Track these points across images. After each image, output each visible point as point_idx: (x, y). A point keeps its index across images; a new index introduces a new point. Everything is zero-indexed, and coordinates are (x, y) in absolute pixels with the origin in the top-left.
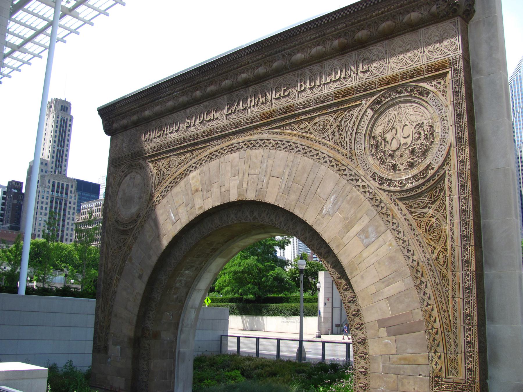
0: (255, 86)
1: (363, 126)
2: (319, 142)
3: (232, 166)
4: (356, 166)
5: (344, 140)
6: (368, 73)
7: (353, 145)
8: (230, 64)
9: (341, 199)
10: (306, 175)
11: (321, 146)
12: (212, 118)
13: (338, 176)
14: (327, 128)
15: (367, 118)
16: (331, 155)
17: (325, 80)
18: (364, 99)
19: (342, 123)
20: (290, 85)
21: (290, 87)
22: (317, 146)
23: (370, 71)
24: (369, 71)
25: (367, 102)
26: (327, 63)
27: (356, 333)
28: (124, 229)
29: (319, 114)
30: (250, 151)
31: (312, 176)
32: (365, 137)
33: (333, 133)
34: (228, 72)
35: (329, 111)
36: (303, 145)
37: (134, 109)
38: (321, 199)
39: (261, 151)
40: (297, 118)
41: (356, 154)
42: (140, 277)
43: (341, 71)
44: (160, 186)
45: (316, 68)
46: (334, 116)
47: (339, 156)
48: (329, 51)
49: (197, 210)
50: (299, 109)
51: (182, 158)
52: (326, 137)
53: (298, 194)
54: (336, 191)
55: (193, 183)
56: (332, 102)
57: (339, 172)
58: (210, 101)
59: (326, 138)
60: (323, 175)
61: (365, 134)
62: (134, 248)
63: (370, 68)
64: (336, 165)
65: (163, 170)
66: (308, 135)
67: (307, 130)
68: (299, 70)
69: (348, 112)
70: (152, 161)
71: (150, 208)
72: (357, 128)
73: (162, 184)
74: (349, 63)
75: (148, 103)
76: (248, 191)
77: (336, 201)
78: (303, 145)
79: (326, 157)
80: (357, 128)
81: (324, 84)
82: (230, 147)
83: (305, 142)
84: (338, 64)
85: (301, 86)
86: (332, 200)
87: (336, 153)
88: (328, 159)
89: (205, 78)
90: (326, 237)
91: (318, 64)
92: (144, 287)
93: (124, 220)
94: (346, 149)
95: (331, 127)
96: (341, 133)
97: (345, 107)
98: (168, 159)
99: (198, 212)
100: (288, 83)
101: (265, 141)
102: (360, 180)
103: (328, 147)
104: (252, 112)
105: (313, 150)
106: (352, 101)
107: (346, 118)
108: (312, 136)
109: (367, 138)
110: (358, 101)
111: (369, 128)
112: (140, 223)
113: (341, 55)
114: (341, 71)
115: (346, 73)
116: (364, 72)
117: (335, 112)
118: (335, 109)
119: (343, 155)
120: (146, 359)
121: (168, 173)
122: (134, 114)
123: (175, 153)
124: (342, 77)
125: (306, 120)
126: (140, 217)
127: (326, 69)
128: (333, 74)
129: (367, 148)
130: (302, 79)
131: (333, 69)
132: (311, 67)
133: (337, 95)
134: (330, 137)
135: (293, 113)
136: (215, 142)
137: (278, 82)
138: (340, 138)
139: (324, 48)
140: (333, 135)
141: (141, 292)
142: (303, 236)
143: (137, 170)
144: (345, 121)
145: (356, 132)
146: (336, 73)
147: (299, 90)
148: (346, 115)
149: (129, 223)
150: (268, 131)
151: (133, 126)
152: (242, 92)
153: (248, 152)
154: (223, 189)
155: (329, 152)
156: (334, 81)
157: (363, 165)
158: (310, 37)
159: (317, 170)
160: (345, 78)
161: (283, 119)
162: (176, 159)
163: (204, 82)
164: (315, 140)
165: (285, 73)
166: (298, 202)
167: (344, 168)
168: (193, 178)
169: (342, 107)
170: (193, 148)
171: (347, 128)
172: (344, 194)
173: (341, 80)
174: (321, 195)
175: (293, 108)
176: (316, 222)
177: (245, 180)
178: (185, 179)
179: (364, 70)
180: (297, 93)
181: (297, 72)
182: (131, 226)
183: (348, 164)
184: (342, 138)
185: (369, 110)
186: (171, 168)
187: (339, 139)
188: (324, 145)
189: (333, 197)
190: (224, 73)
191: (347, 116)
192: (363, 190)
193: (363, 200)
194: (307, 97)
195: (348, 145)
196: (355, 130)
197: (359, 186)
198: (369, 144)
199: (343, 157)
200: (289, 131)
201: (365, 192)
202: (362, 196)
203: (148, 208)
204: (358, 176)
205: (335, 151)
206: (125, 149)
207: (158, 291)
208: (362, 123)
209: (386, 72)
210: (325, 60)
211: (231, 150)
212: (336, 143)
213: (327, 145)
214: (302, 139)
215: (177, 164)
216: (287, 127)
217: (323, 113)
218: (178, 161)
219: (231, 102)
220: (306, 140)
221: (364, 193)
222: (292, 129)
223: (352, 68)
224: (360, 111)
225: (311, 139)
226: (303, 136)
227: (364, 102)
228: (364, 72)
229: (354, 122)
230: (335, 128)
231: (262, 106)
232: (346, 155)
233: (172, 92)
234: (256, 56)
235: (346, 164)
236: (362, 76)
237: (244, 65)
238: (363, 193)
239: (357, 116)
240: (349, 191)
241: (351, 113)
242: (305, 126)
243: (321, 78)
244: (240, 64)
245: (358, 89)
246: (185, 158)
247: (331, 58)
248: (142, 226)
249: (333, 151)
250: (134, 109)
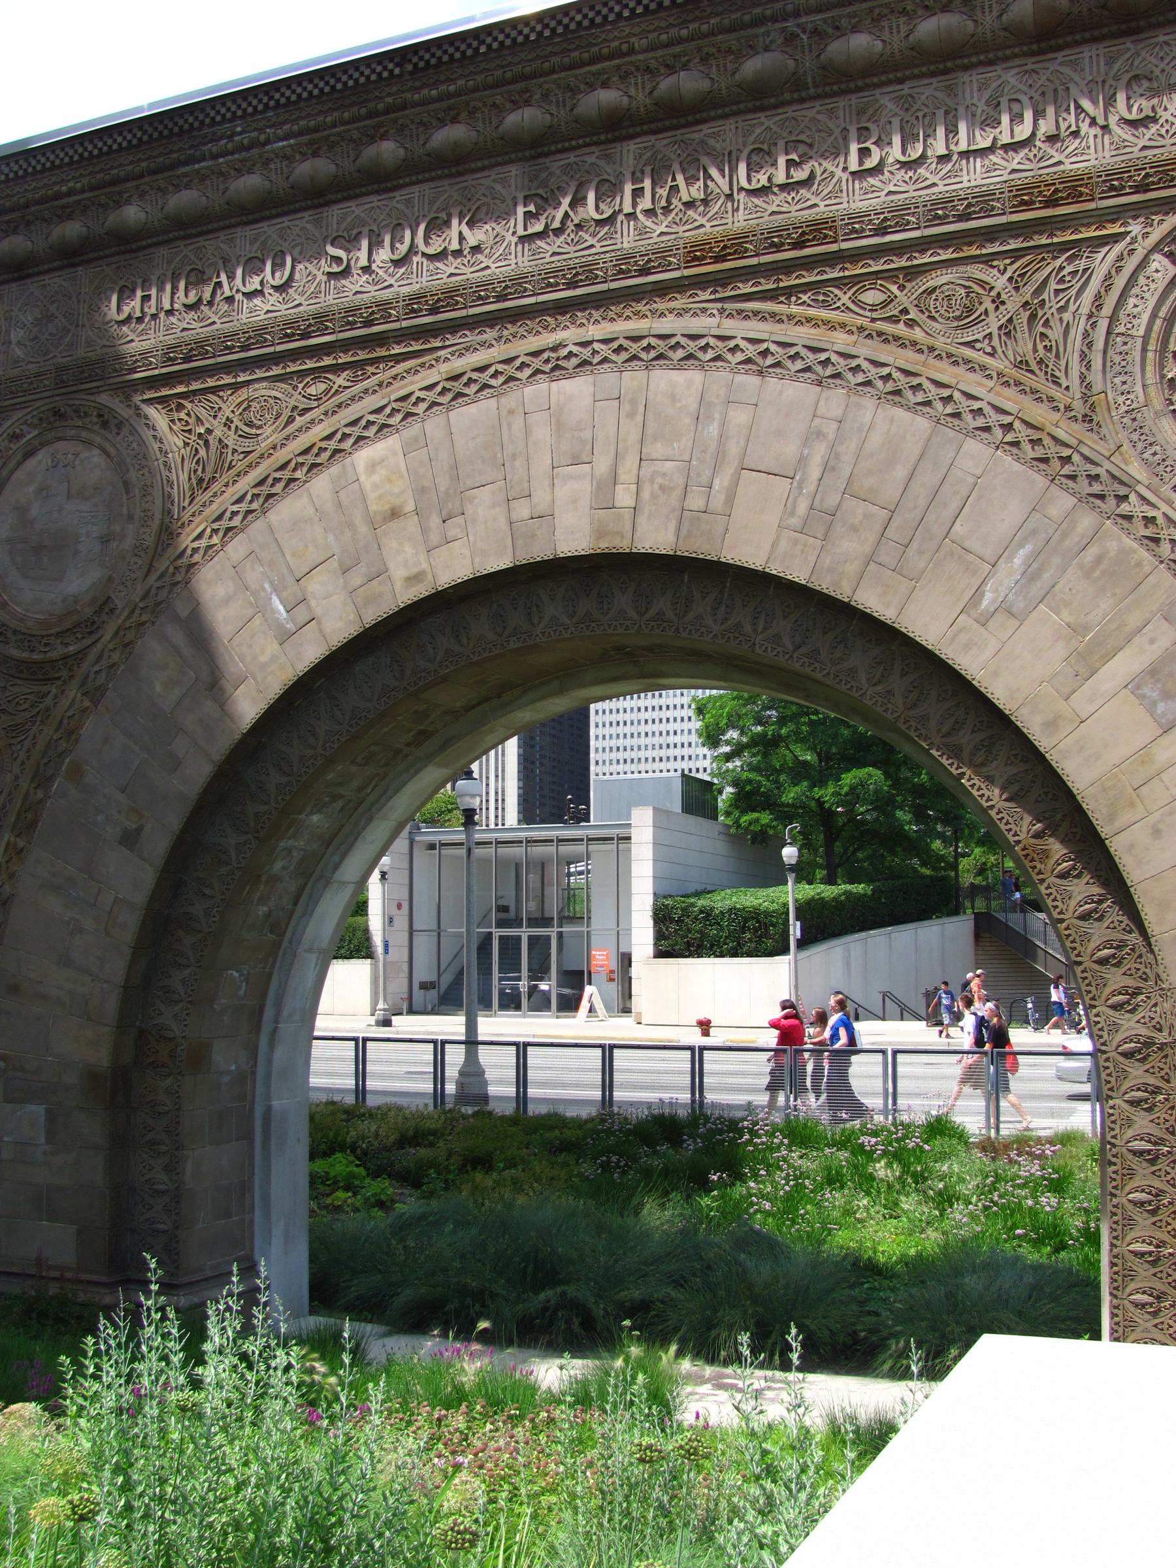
0: (652, 138)
1: (1135, 311)
2: (950, 355)
3: (559, 427)
4: (1113, 447)
5: (1057, 356)
6: (1154, 128)
7: (1095, 377)
8: (549, 49)
9: (1056, 560)
10: (900, 473)
11: (961, 370)
12: (455, 246)
13: (1040, 481)
14: (981, 309)
15: (1153, 286)
16: (1008, 406)
17: (971, 139)
18: (1135, 218)
19: (1045, 296)
20: (811, 146)
21: (811, 153)
22: (946, 372)
23: (1161, 121)
24: (1154, 120)
25: (1148, 229)
26: (974, 78)
27: (1115, 1024)
28: (35, 656)
29: (944, 257)
30: (642, 374)
31: (927, 479)
32: (1144, 350)
33: (1008, 330)
34: (533, 76)
35: (990, 251)
36: (884, 365)
37: (69, 194)
38: (970, 557)
39: (695, 377)
40: (848, 265)
41: (1113, 406)
42: (130, 839)
43: (1038, 114)
44: (210, 493)
45: (927, 91)
46: (1010, 270)
47: (1040, 411)
48: (989, 35)
49: (399, 586)
50: (859, 234)
51: (312, 390)
52: (977, 341)
53: (871, 537)
54: (1034, 533)
55: (376, 487)
56: (1003, 220)
57: (1042, 466)
58: (439, 183)
59: (978, 346)
60: (978, 472)
61: (1146, 338)
62: (90, 728)
63: (1160, 112)
64: (1031, 441)
65: (218, 433)
66: (900, 329)
67: (896, 312)
68: (853, 97)
69: (1070, 259)
70: (162, 400)
71: (161, 576)
72: (1113, 318)
73: (215, 487)
74: (1072, 86)
75: (142, 176)
76: (642, 521)
77: (1035, 566)
78: (884, 365)
79: (987, 410)
80: (1113, 318)
81: (966, 155)
82: (545, 356)
83: (886, 354)
84: (1021, 86)
85: (864, 153)
86: (1017, 561)
87: (1027, 401)
88: (993, 418)
89: (425, 92)
90: (999, 692)
91: (934, 80)
92: (149, 876)
93: (30, 623)
94: (1067, 388)
95: (997, 308)
96: (1043, 330)
97: (1055, 240)
98: (243, 394)
99: (406, 596)
100: (802, 137)
101: (712, 341)
102: (1133, 497)
103: (989, 377)
104: (642, 232)
105: (927, 384)
106: (1086, 221)
107: (1061, 281)
108: (918, 334)
109: (1150, 355)
110: (1108, 225)
111: (1158, 322)
112: (117, 633)
113: (1033, 54)
114: (1038, 114)
115: (1057, 122)
116: (1133, 124)
117: (1016, 254)
118: (1013, 245)
119: (1056, 409)
120: (163, 1148)
121: (247, 445)
122: (66, 214)
123: (276, 371)
124: (1040, 134)
125: (889, 275)
126: (112, 611)
127: (968, 102)
128: (1005, 119)
129: (1152, 391)
130: (867, 129)
131: (1004, 101)
132: (906, 88)
133: (1023, 196)
134: (995, 342)
135: (834, 247)
136: (472, 337)
137: (758, 131)
138: (1040, 347)
139: (970, 23)
140: (1008, 334)
141: (140, 898)
142: (879, 688)
143: (84, 434)
144: (1057, 292)
145: (1109, 333)
146: (1017, 118)
147: (854, 166)
148: (1061, 268)
149: (58, 635)
150: (719, 305)
151: (56, 264)
152: (590, 159)
153: (633, 379)
154: (522, 510)
155: (998, 394)
156: (1006, 147)
157: (1140, 445)
158: (655, 35)
159: (952, 455)
160: (1052, 139)
161: (788, 267)
162: (279, 395)
163: (418, 109)
164: (932, 349)
165: (789, 103)
166: (872, 566)
167: (1066, 452)
168: (372, 466)
169: (1044, 241)
170: (362, 355)
171: (1067, 316)
172: (1068, 543)
173: (1038, 143)
174: (971, 544)
175: (830, 228)
176: (955, 636)
177: (622, 477)
178: (334, 470)
179: (1134, 116)
180: (845, 176)
181: (842, 102)
182: (67, 645)
183: (1080, 442)
184: (1048, 349)
185: (1157, 256)
186: (259, 427)
187: (1035, 350)
188: (972, 369)
189: (1021, 552)
190: (514, 81)
191: (1065, 272)
192: (1148, 533)
193: (1147, 569)
194: (890, 193)
195: (1075, 372)
196: (1103, 325)
197: (1128, 518)
198: (1162, 376)
199: (1056, 416)
200: (812, 312)
201: (1156, 541)
202: (1143, 553)
203: (153, 577)
204: (1122, 483)
205: (1023, 392)
206: (20, 353)
207: (208, 891)
208: (1132, 301)
209: (1093, 156)
210: (966, 68)
211: (553, 370)
212: (1023, 365)
213: (983, 368)
214: (875, 343)
215: (286, 413)
216: (804, 298)
217: (961, 255)
218: (293, 403)
219: (540, 191)
220: (891, 347)
221: (1151, 545)
222: (825, 305)
223: (1086, 104)
224: (1120, 258)
225: (914, 343)
226: (880, 334)
227: (1135, 228)
228: (1133, 124)
229: (1098, 296)
230: (1017, 313)
231: (690, 213)
232: (1068, 408)
233: (262, 138)
234: (671, 26)
235: (1074, 442)
236: (1125, 137)
237: (611, 57)
238: (1146, 541)
239: (1108, 276)
240: (1090, 533)
241: (1082, 264)
242: (882, 297)
243: (952, 131)
244: (595, 49)
245: (1113, 182)
246: (327, 391)
247: (991, 63)
248: (126, 645)
249: (1011, 392)
250: (69, 194)
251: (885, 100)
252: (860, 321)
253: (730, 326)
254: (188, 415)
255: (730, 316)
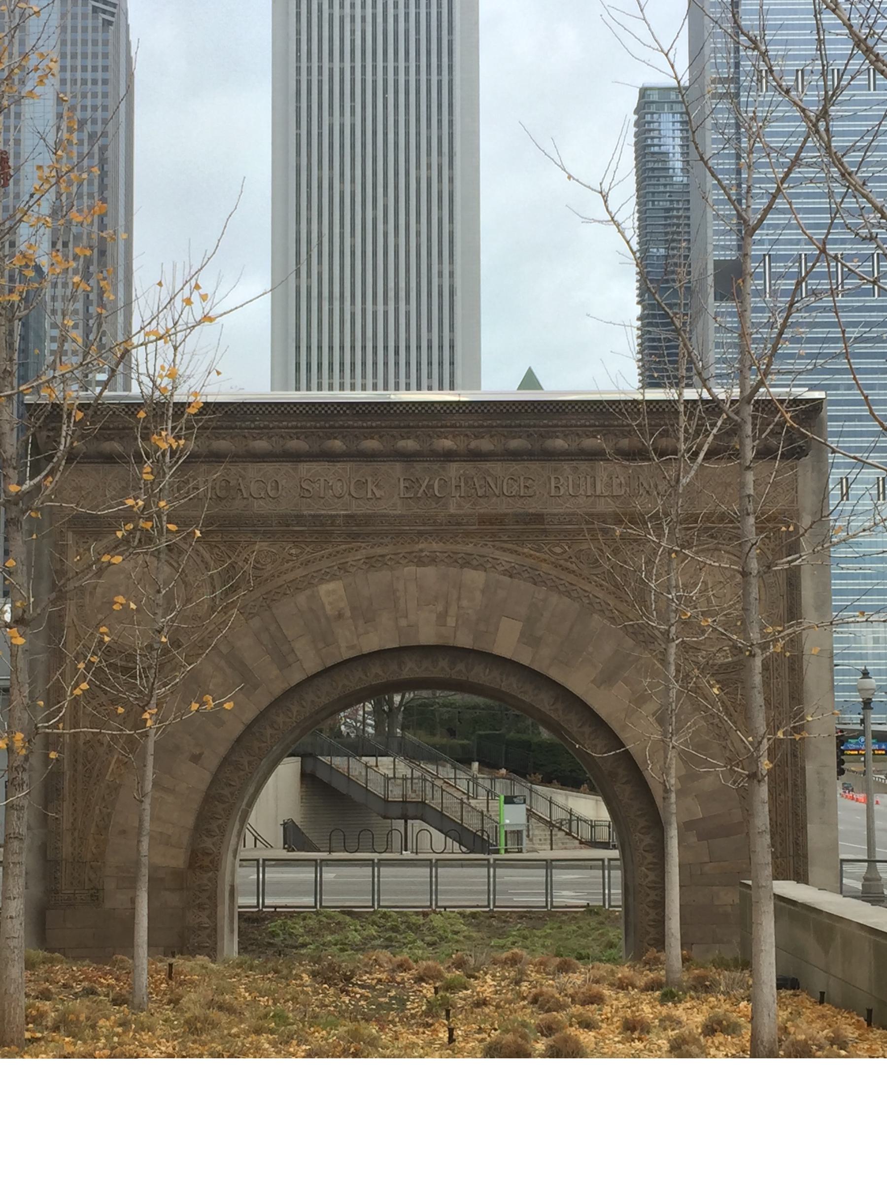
34: (412, 427)
42: (196, 759)
55: (330, 604)
82: (414, 554)
92: (208, 777)
137: (512, 470)
141: (203, 787)
178: (308, 592)
181: (548, 464)
190: (404, 427)
200: (532, 552)
207: (233, 783)
233: (271, 426)
237: (451, 427)
246: (301, 553)
251: (566, 467)
252: (553, 560)
253: (498, 554)
254: (222, 552)
255: (497, 549)
